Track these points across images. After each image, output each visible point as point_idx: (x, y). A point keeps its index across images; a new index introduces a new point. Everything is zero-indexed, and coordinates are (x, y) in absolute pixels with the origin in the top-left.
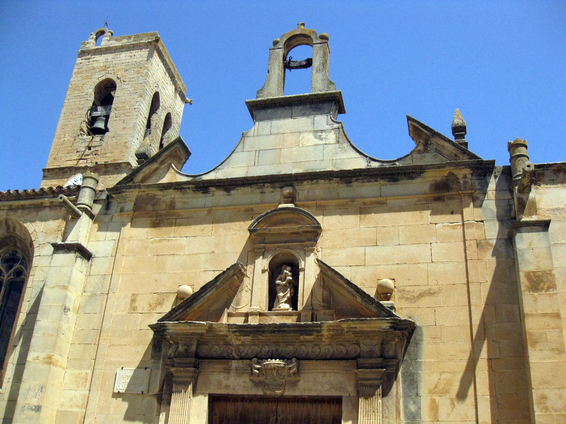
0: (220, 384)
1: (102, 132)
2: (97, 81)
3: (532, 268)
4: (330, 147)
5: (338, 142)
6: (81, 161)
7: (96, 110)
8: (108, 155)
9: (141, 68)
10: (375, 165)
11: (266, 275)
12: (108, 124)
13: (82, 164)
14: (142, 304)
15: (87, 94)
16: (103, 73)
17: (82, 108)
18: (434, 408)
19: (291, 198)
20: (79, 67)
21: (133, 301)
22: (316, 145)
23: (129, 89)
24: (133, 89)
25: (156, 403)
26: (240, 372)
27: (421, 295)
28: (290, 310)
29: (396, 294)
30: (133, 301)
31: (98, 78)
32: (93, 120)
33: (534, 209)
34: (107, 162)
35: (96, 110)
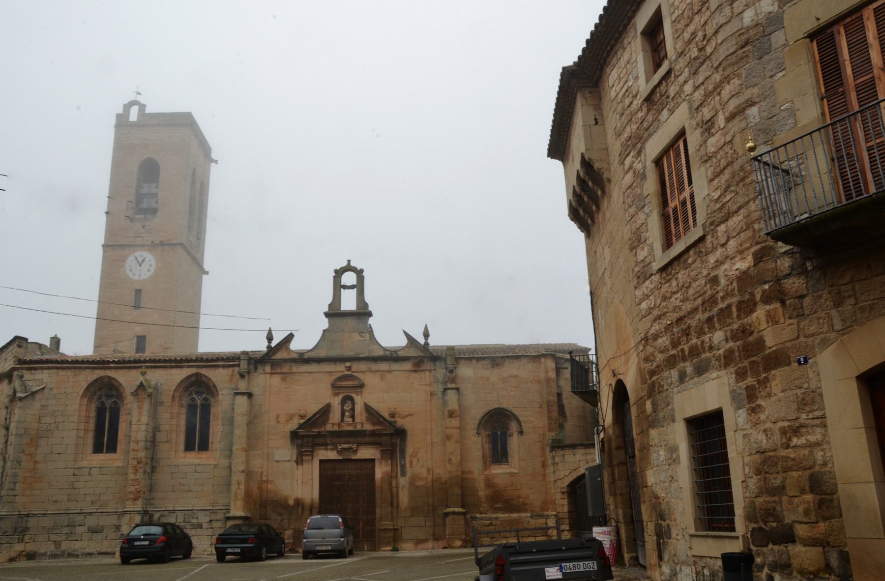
0: (324, 455)
3: (450, 408)
4: (367, 342)
5: (370, 339)
6: (138, 239)
11: (340, 406)
14: (282, 419)
18: (411, 462)
19: (349, 369)
22: (360, 340)
26: (332, 450)
27: (407, 416)
28: (351, 422)
29: (397, 416)
34: (162, 242)
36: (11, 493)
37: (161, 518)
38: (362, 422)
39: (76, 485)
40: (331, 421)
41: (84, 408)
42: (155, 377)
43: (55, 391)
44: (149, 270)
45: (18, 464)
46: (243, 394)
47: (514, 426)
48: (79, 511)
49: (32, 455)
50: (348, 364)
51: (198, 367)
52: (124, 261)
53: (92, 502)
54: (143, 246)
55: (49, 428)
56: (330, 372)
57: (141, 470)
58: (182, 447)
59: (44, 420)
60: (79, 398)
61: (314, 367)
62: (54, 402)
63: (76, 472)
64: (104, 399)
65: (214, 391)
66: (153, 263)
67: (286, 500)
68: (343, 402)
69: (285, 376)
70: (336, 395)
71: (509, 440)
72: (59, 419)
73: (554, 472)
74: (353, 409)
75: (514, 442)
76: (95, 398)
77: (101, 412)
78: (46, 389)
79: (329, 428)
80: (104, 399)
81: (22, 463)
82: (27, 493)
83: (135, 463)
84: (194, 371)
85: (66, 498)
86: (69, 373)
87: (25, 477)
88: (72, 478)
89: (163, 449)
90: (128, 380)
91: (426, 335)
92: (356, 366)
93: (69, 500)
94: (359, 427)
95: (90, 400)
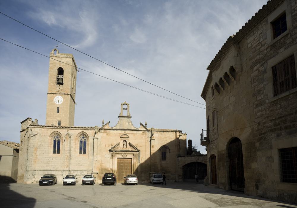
1: (62, 84)
10: (136, 129)
13: (58, 93)
18: (141, 159)
21: (106, 145)
25: (110, 159)
30: (106, 145)
32: (58, 79)
33: (153, 138)
36: (30, 164)
38: (129, 148)
40: (120, 147)
42: (71, 132)
43: (41, 135)
44: (61, 102)
46: (96, 138)
47: (168, 151)
50: (125, 131)
51: (83, 130)
56: (120, 133)
57: (68, 159)
58: (79, 153)
61: (116, 131)
62: (41, 138)
65: (88, 137)
66: (62, 99)
67: (108, 168)
68: (124, 141)
69: (107, 134)
70: (121, 140)
71: (166, 154)
72: (43, 143)
73: (178, 163)
74: (126, 144)
75: (168, 155)
76: (53, 137)
77: (55, 141)
79: (119, 149)
82: (35, 164)
83: (66, 157)
84: (82, 131)
85: (46, 166)
87: (34, 160)
89: (73, 153)
90: (63, 132)
91: (146, 125)
92: (127, 132)
93: (47, 167)
94: (128, 149)
95: (52, 138)
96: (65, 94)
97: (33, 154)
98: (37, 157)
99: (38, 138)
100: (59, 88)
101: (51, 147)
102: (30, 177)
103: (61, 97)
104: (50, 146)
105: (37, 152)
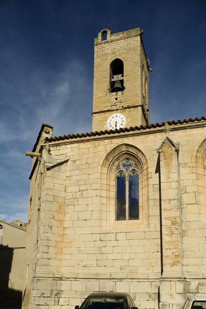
1: (122, 89)
2: (111, 61)
7: (113, 78)
8: (129, 102)
9: (135, 51)
12: (124, 84)
13: (114, 108)
15: (106, 69)
16: (113, 56)
17: (106, 77)
20: (97, 54)
23: (131, 64)
24: (134, 63)
31: (111, 59)
32: (112, 84)
35: (113, 78)
37: (200, 286)
39: (104, 250)
41: (105, 176)
43: (78, 163)
45: (50, 229)
48: (109, 277)
49: (61, 221)
52: (106, 121)
53: (121, 269)
54: (117, 110)
55: (74, 196)
59: (69, 189)
60: (100, 167)
62: (78, 172)
63: (103, 238)
64: (122, 168)
66: (124, 119)
72: (82, 188)
76: (114, 168)
77: (120, 181)
78: (69, 161)
80: (122, 168)
81: (53, 228)
82: (59, 257)
86: (89, 145)
88: (99, 244)
93: (97, 265)
95: (110, 169)
96: (129, 107)
97: (54, 223)
98: (67, 232)
99: (68, 174)
100: (116, 99)
101: (108, 198)
102: (43, 301)
103: (122, 116)
104: (104, 194)
105: (67, 217)
